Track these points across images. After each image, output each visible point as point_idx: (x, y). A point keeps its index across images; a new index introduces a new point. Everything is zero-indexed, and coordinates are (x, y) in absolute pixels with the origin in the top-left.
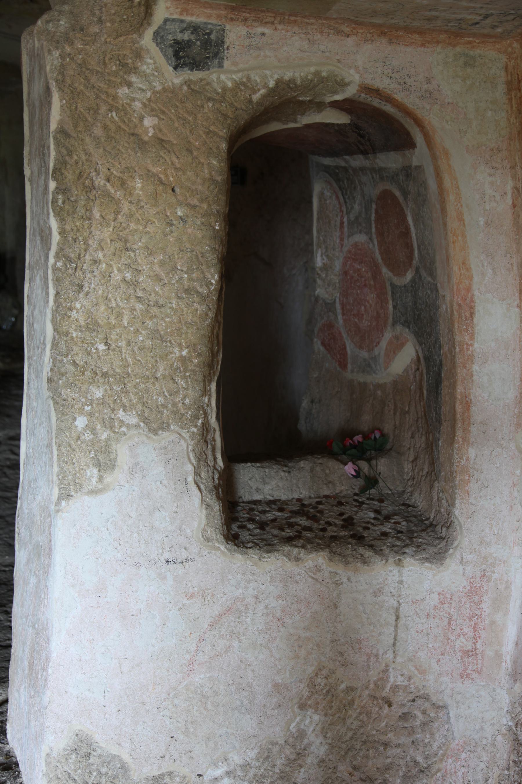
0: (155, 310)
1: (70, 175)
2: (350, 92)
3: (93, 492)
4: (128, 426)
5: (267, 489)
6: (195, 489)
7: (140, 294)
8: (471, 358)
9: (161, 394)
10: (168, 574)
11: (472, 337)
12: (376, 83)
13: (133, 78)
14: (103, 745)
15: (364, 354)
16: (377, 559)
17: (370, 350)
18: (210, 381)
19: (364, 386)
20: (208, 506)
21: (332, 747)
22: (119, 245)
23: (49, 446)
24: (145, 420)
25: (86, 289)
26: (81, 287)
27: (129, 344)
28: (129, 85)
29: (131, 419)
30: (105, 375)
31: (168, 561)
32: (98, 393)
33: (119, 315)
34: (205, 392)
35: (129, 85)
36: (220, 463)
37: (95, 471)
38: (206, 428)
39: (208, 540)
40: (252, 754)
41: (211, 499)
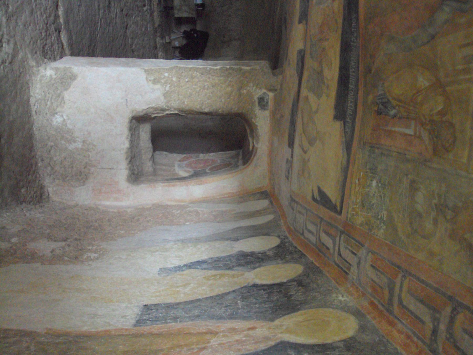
0: (197, 94)
1: (231, 71)
2: (256, 146)
3: (147, 79)
4: (165, 88)
5: (143, 133)
6: (147, 107)
7: (201, 90)
8: (187, 186)
9: (174, 97)
10: (123, 100)
11: (193, 185)
12: (258, 151)
13: (255, 87)
14: (74, 83)
15: (184, 166)
16: (128, 162)
17: (185, 166)
18: (177, 111)
19: (174, 166)
20: (142, 111)
21: (71, 151)
22: (214, 84)
23: (158, 66)
24: (167, 92)
25: (202, 76)
26: (202, 74)
27: (188, 87)
28: (253, 86)
29: (167, 88)
30: (179, 81)
31: (127, 100)
32: (174, 79)
33: (196, 85)
34: (175, 109)
35: (253, 86)
36: (153, 116)
37: (153, 79)
38: (163, 110)
39: (133, 111)
40: (70, 127)
41: (144, 112)
